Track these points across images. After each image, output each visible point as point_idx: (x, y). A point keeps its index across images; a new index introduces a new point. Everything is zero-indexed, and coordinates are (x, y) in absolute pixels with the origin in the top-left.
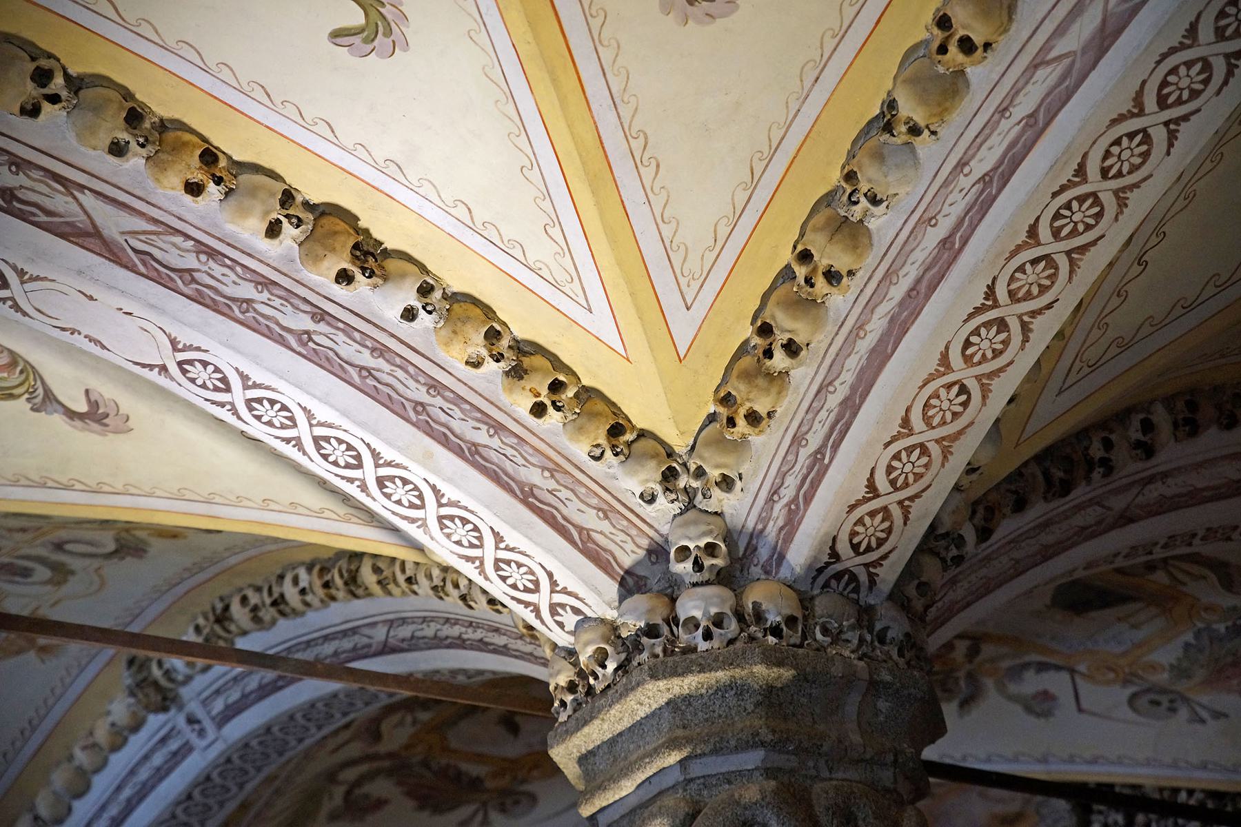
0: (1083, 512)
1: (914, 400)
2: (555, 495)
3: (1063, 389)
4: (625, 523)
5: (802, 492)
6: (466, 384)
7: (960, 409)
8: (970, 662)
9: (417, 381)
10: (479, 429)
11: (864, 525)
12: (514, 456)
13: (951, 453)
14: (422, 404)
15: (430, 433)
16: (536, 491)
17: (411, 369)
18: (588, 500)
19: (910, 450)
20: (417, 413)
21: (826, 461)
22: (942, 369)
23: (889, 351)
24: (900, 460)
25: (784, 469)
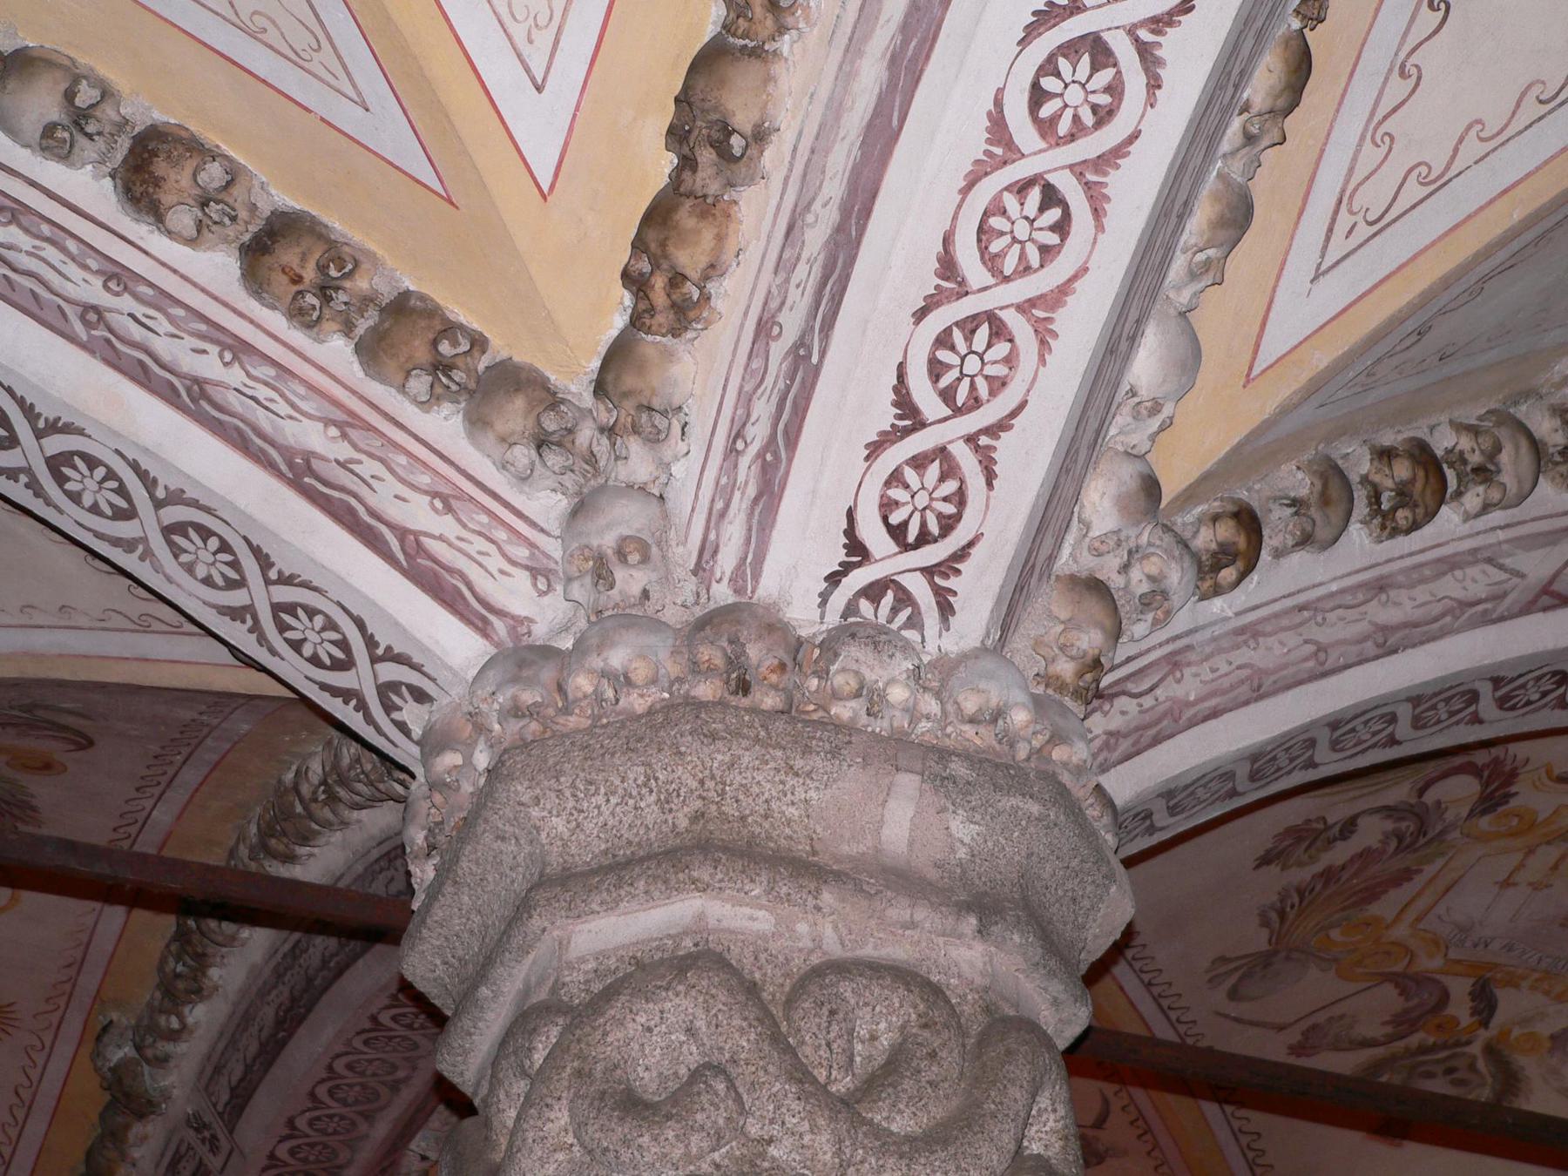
0: (1458, 573)
1: (955, 218)
2: (352, 471)
3: (1323, 268)
4: (484, 519)
5: (781, 426)
6: (175, 271)
7: (1052, 239)
8: (1485, 1024)
9: (85, 267)
10: (204, 352)
11: (907, 487)
12: (272, 400)
13: (1055, 335)
14: (95, 309)
15: (115, 362)
16: (315, 464)
17: (72, 245)
18: (411, 478)
19: (970, 326)
20: (87, 324)
21: (815, 360)
22: (998, 151)
23: (895, 122)
24: (953, 348)
25: (748, 388)
